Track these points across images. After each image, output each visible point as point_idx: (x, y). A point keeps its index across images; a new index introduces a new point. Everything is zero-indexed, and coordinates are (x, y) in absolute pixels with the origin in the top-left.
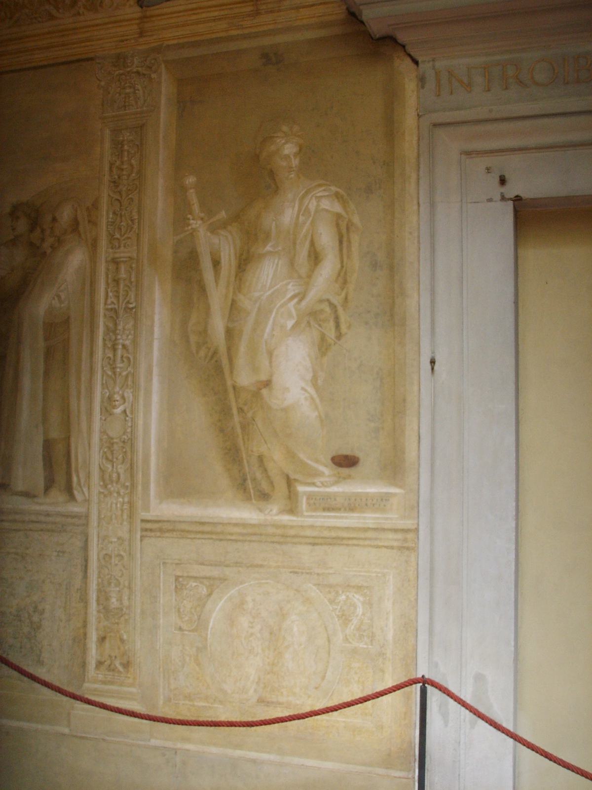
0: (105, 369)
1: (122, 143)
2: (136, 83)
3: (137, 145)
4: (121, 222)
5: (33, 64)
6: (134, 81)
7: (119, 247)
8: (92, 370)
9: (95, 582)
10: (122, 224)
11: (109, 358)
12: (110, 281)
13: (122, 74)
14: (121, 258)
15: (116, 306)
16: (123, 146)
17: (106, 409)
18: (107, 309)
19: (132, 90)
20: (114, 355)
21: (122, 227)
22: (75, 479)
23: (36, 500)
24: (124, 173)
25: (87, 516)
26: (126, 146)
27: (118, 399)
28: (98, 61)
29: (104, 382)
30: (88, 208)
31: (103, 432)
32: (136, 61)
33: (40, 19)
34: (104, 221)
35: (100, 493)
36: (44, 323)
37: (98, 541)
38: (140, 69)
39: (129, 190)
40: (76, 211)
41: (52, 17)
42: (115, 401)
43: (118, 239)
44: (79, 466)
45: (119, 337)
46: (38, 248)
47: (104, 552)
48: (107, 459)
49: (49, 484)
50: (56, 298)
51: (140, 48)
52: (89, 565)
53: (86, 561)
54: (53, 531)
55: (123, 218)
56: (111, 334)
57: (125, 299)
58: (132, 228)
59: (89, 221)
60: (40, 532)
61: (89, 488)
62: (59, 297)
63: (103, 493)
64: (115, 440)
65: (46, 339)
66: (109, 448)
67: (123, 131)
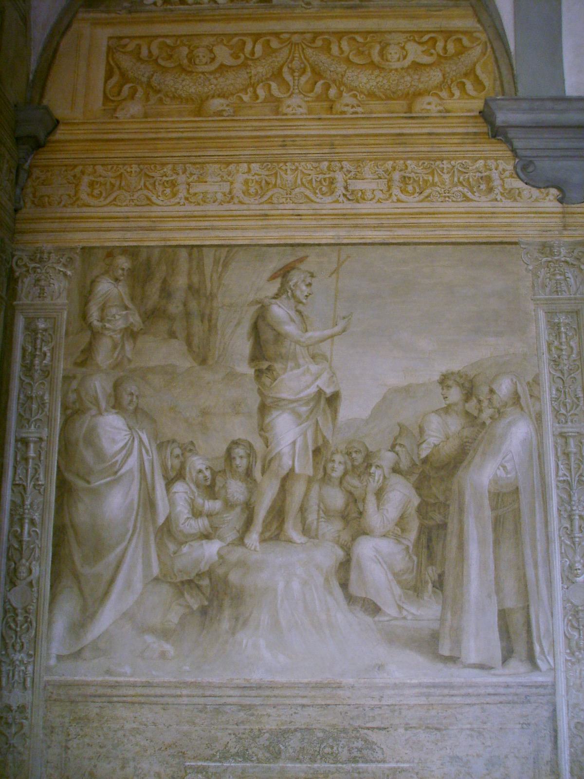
0: (562, 538)
1: (558, 325)
2: (566, 271)
3: (574, 328)
4: (566, 399)
5: (453, 240)
6: (564, 270)
7: (566, 422)
8: (548, 540)
9: (567, 753)
10: (567, 400)
11: (567, 528)
12: (559, 454)
13: (550, 262)
14: (568, 432)
15: (569, 479)
16: (559, 328)
17: (567, 577)
18: (559, 481)
19: (562, 277)
20: (572, 525)
21: (568, 405)
22: (537, 648)
23: (493, 672)
24: (564, 353)
25: (554, 685)
26: (562, 328)
27: (580, 567)
28: (522, 246)
29: (563, 551)
30: (528, 383)
31: (566, 600)
32: (563, 251)
33: (454, 199)
34: (547, 397)
35: (566, 660)
36: (489, 492)
37: (568, 709)
38: (568, 259)
39: (571, 369)
40: (516, 385)
41: (468, 200)
42: (576, 570)
43: (563, 414)
44: (542, 635)
45: (574, 508)
46: (476, 418)
47: (576, 721)
48: (573, 626)
49: (508, 654)
50: (501, 468)
51: (566, 239)
52: (559, 735)
53: (555, 730)
54: (514, 703)
55: (567, 396)
56: (566, 505)
57: (578, 471)
58: (578, 405)
59: (531, 396)
60: (499, 705)
61: (554, 657)
62: (504, 467)
63: (570, 660)
64: (580, 608)
65: (493, 509)
66: (574, 616)
67: (558, 314)
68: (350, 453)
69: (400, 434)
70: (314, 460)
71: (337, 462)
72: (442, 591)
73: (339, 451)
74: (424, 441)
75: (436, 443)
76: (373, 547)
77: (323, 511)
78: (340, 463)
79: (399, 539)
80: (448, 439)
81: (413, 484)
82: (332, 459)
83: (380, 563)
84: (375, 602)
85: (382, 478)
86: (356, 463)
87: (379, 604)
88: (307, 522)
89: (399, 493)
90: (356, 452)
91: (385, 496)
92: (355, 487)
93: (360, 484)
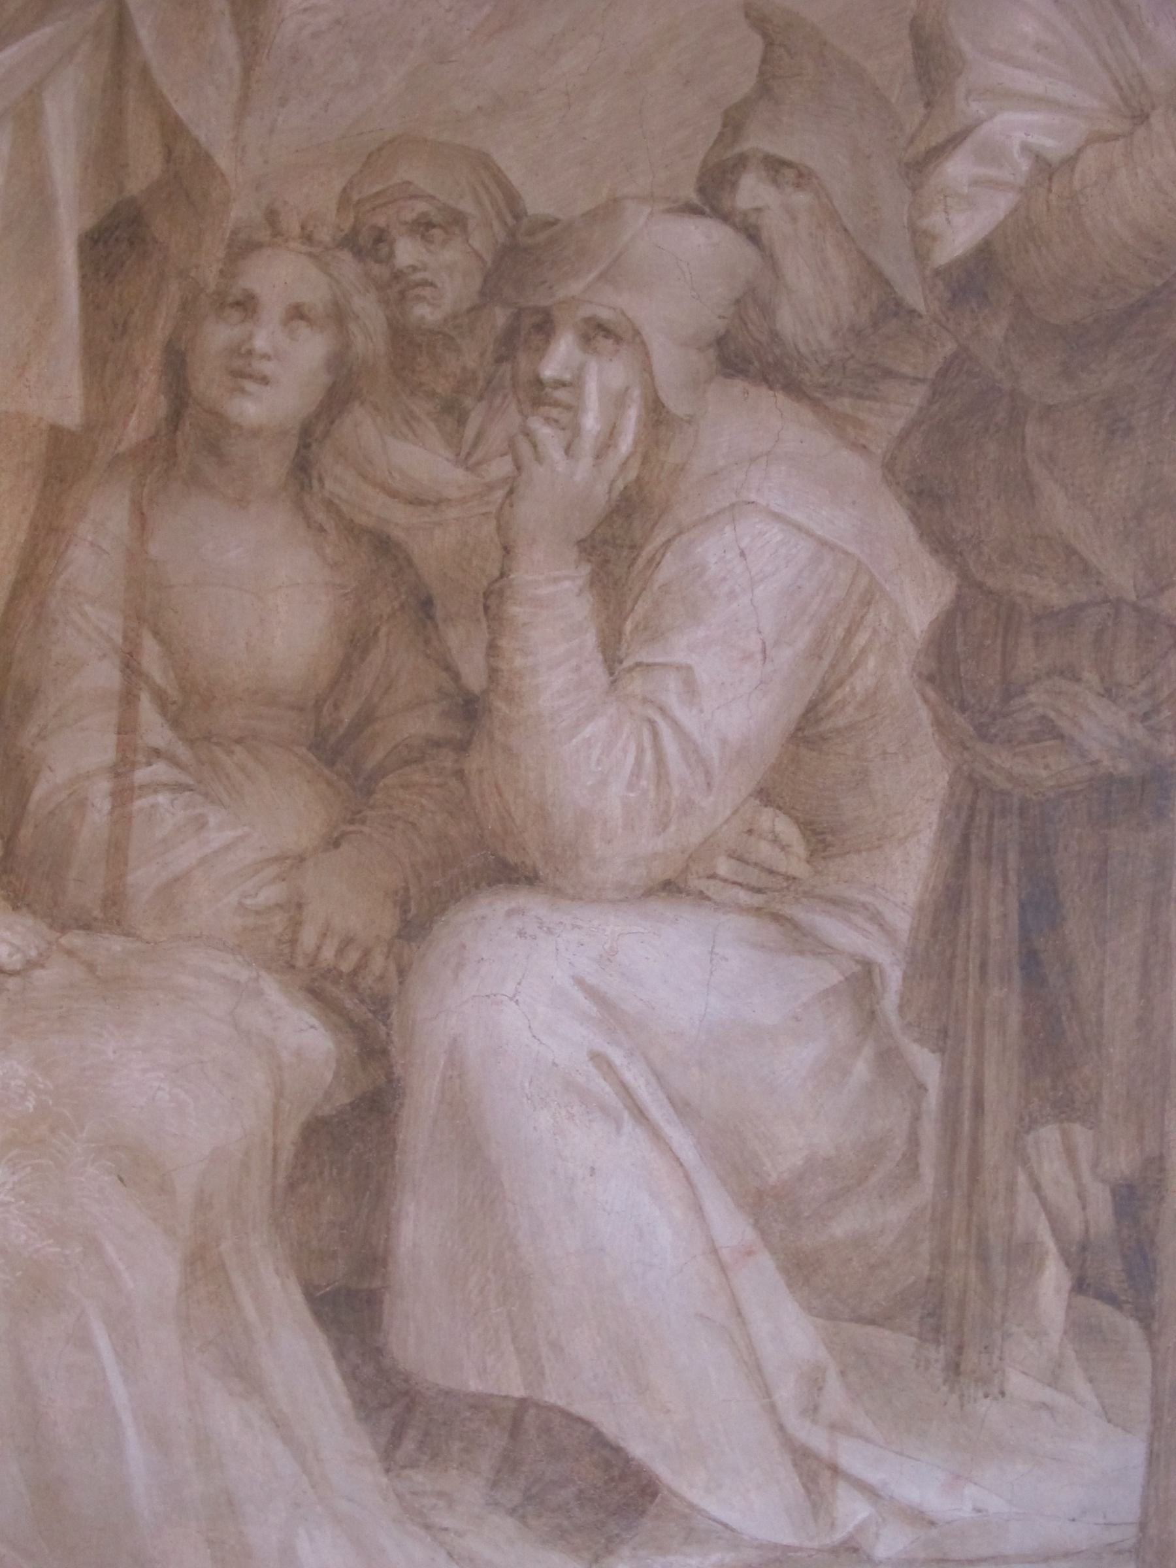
68: (381, 237)
69: (764, 89)
70: (92, 305)
71: (273, 309)
72: (1146, 1317)
73: (291, 224)
74: (955, 140)
75: (1053, 146)
76: (580, 982)
77: (161, 700)
78: (297, 313)
79: (799, 913)
80: (1141, 117)
81: (889, 466)
82: (236, 293)
83: (640, 1114)
84: (609, 1427)
85: (633, 414)
86: (425, 313)
87: (638, 1450)
88: (38, 793)
89: (775, 533)
90: (423, 227)
91: (668, 569)
92: (417, 502)
93: (459, 474)
